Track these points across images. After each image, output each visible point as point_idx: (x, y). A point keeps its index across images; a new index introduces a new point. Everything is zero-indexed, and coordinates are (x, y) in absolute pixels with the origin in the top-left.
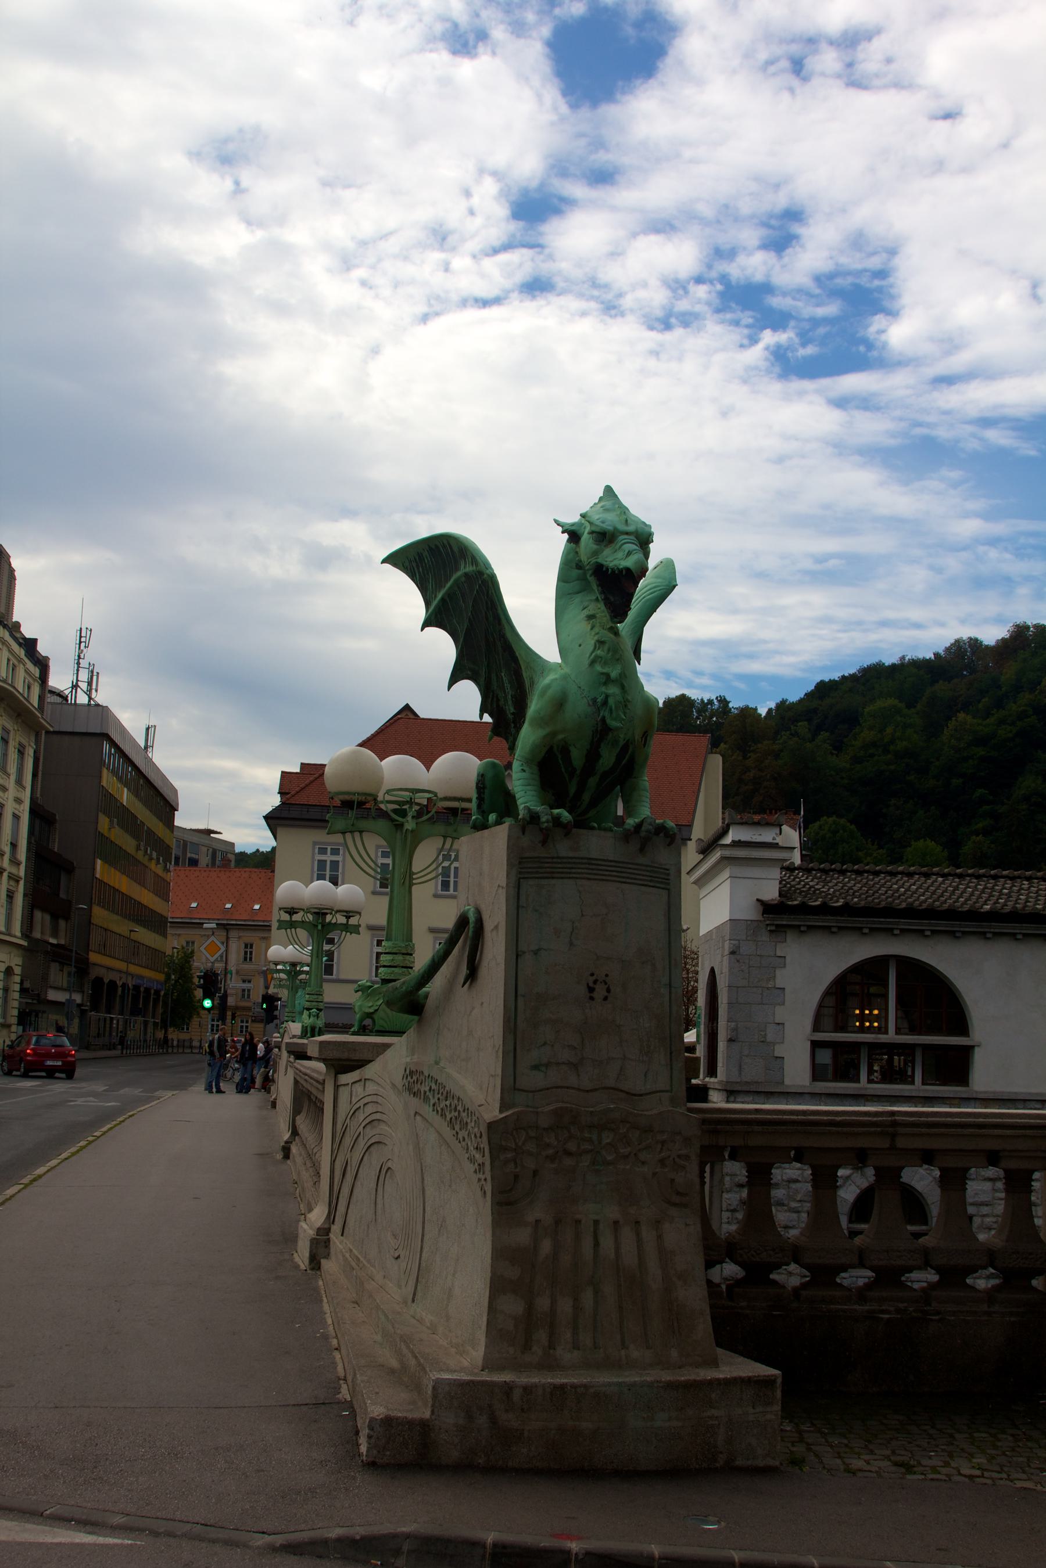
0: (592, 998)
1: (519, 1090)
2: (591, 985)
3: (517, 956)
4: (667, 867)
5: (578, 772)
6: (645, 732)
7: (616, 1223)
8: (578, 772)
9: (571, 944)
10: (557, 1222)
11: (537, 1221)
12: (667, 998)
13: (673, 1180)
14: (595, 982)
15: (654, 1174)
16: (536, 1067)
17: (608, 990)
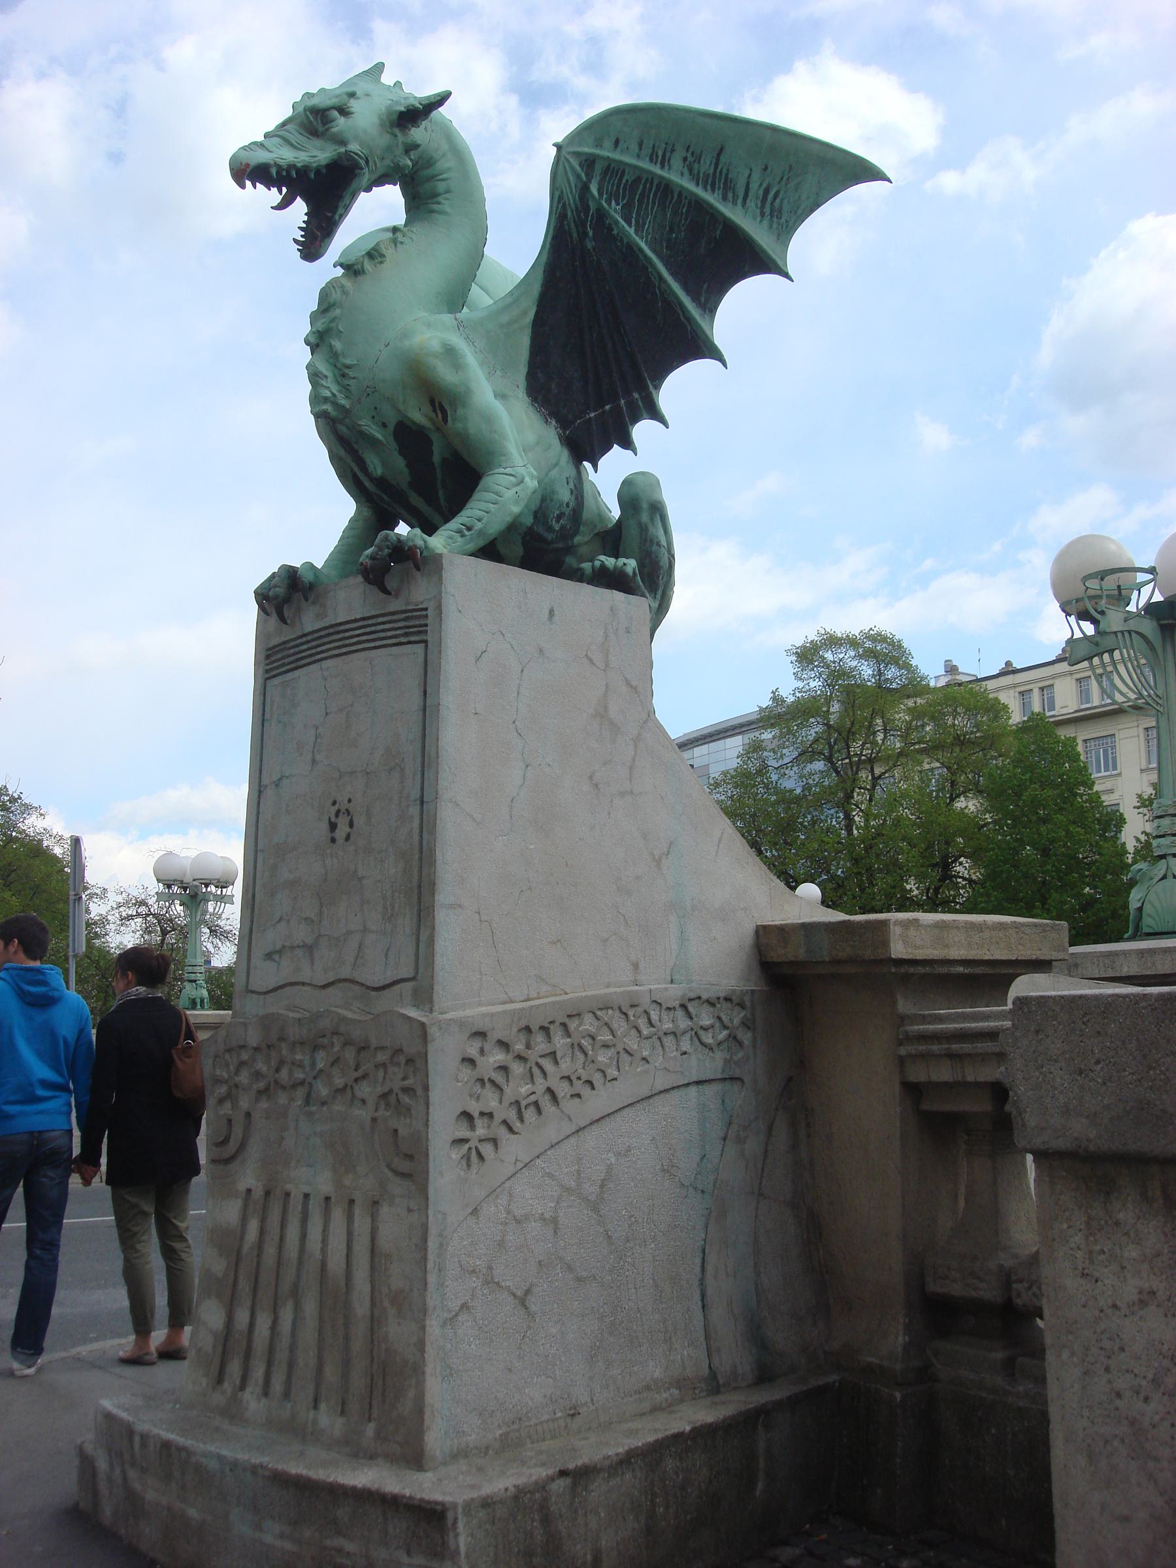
0: (333, 840)
1: (253, 992)
2: (333, 819)
3: (260, 792)
4: (424, 606)
5: (385, 497)
6: (432, 402)
7: (328, 1199)
8: (385, 497)
9: (314, 761)
10: (267, 1194)
11: (249, 1191)
12: (416, 823)
13: (396, 1131)
14: (337, 815)
15: (374, 1120)
16: (269, 956)
17: (351, 825)
